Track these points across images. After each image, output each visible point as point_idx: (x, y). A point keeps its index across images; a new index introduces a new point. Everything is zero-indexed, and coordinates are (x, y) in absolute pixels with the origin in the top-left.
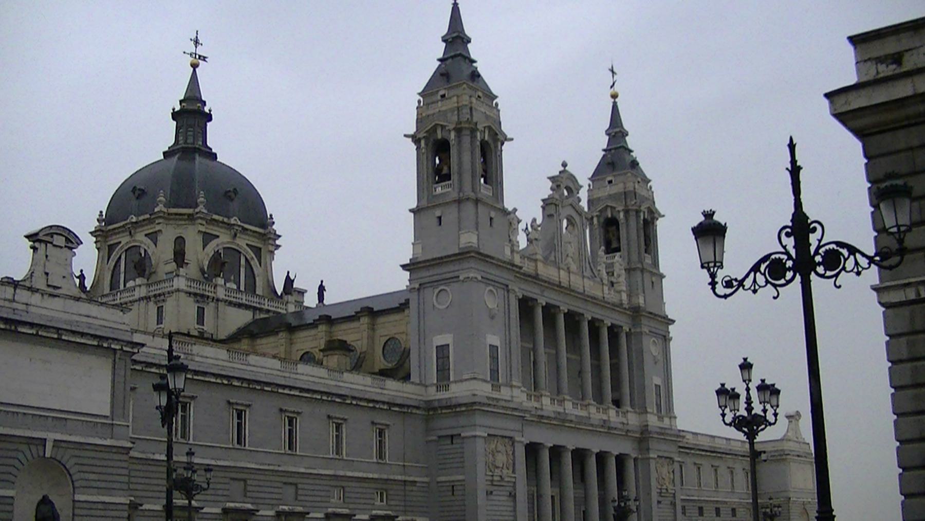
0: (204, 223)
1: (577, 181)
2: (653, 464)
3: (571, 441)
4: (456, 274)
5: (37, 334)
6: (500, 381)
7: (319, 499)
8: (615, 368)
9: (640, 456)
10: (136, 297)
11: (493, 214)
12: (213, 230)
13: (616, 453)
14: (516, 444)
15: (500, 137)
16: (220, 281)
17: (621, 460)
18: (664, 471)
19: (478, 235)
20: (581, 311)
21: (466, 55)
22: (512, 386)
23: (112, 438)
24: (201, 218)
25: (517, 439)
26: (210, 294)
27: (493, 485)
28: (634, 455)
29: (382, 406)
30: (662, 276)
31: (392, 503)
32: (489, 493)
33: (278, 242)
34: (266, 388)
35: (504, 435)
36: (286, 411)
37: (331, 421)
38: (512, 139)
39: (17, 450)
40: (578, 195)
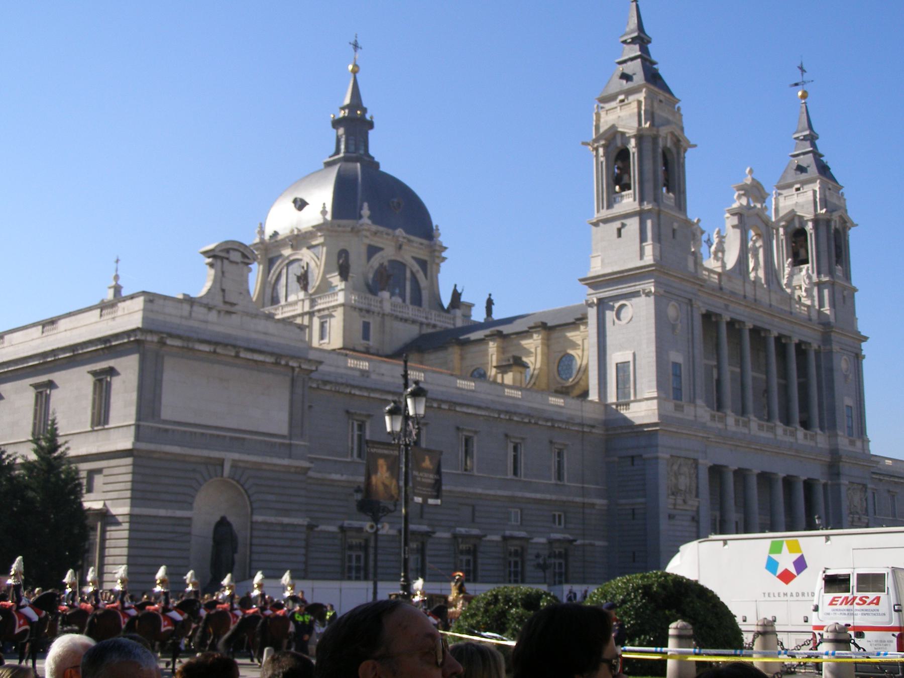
0: (368, 234)
1: (763, 189)
2: (843, 489)
3: (756, 464)
4: (637, 288)
5: (215, 352)
8: (804, 389)
9: (830, 482)
10: (299, 311)
11: (676, 226)
12: (376, 242)
13: (803, 478)
14: (700, 466)
15: (683, 144)
16: (386, 295)
17: (809, 485)
18: (857, 498)
19: (661, 248)
20: (767, 327)
21: (645, 56)
22: (695, 406)
23: (290, 457)
24: (368, 230)
25: (701, 461)
26: (376, 309)
27: (675, 509)
28: (823, 481)
29: (560, 425)
30: (855, 290)
33: (444, 254)
36: (463, 430)
38: (695, 146)
39: (194, 471)
40: (764, 205)
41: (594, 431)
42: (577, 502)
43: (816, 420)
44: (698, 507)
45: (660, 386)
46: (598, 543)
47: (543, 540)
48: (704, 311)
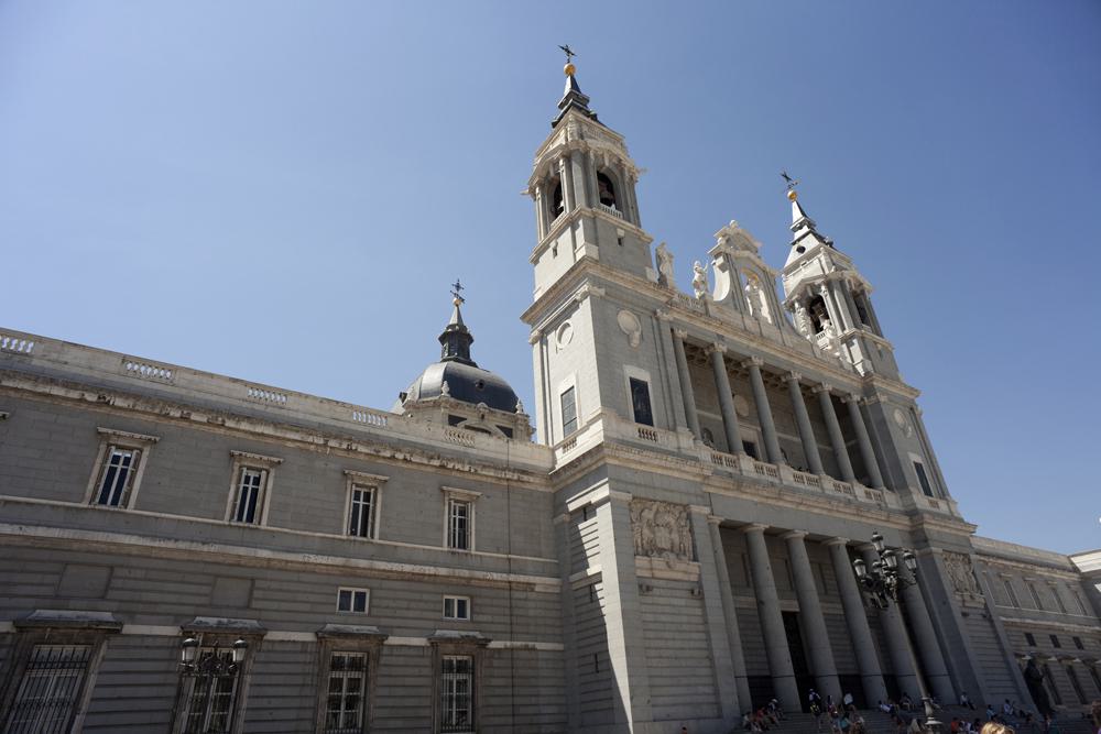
6: (655, 423)
7: (307, 607)
9: (916, 552)
11: (621, 233)
12: (458, 413)
14: (693, 516)
18: (961, 570)
20: (787, 369)
25: (695, 509)
29: (458, 466)
31: (476, 618)
32: (644, 588)
34: (194, 417)
35: (670, 500)
37: (349, 482)
38: (645, 170)
41: (525, 478)
42: (496, 581)
43: (879, 479)
44: (700, 575)
45: (606, 400)
46: (539, 646)
47: (421, 641)
48: (681, 334)
